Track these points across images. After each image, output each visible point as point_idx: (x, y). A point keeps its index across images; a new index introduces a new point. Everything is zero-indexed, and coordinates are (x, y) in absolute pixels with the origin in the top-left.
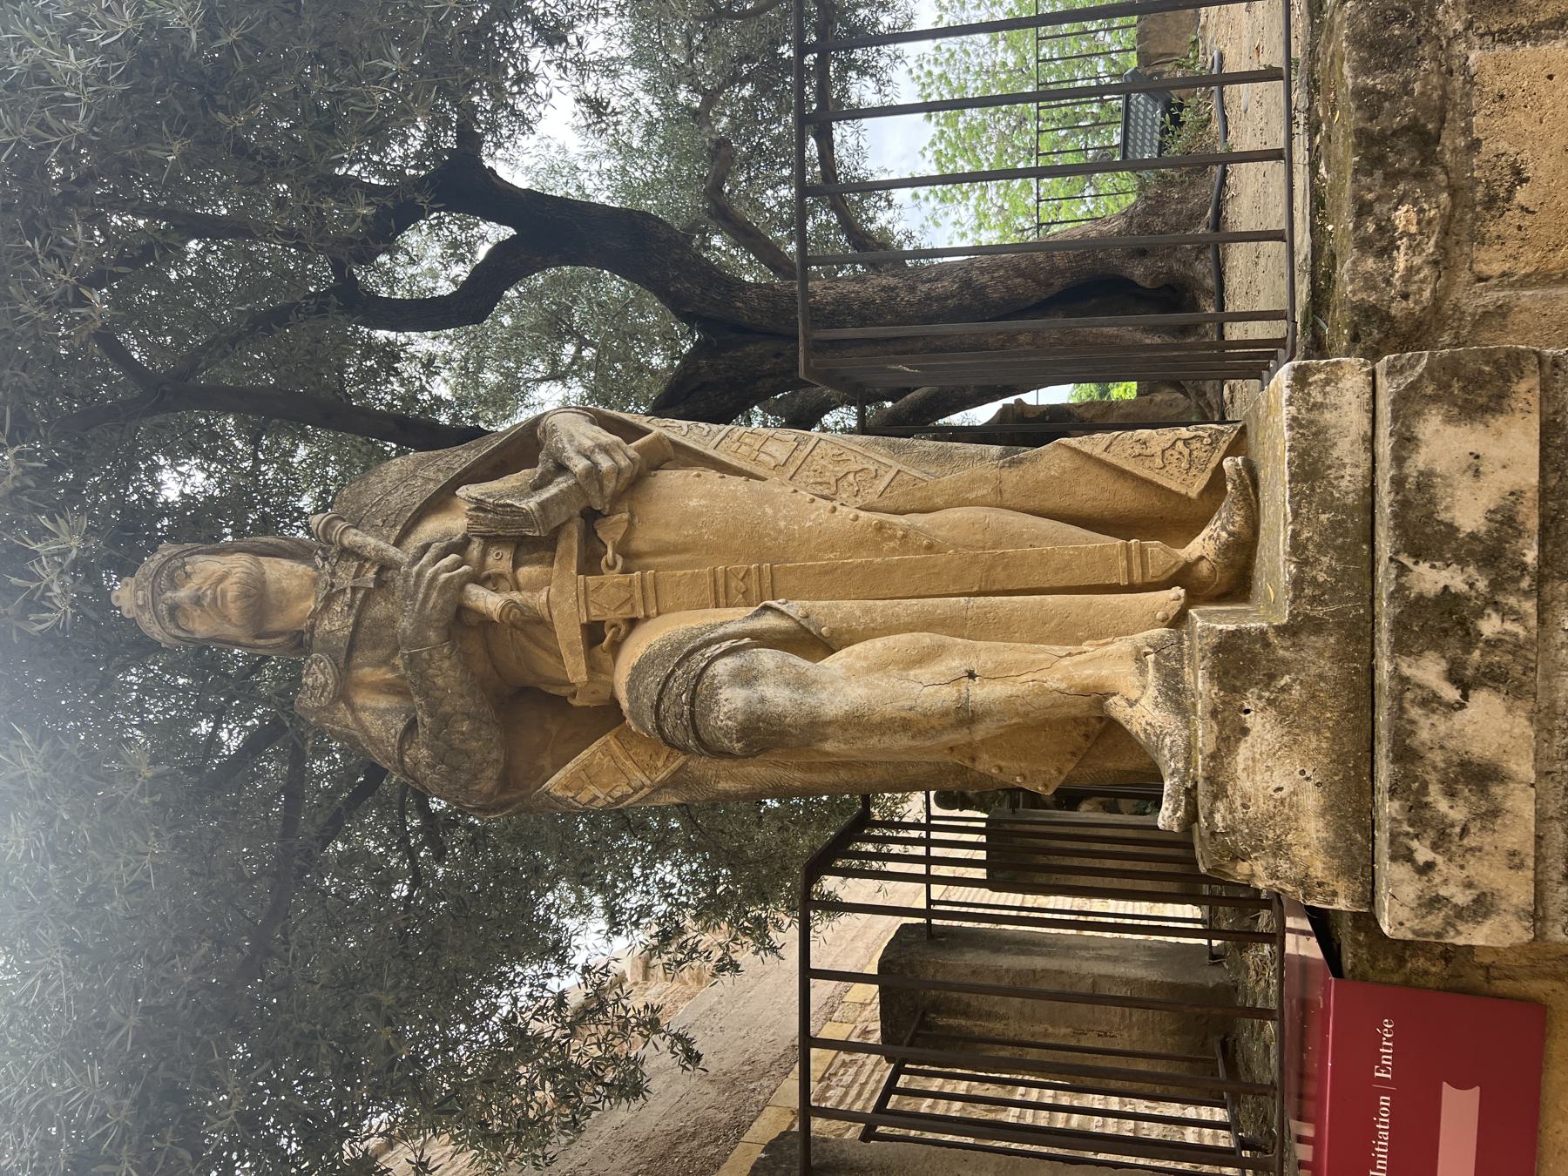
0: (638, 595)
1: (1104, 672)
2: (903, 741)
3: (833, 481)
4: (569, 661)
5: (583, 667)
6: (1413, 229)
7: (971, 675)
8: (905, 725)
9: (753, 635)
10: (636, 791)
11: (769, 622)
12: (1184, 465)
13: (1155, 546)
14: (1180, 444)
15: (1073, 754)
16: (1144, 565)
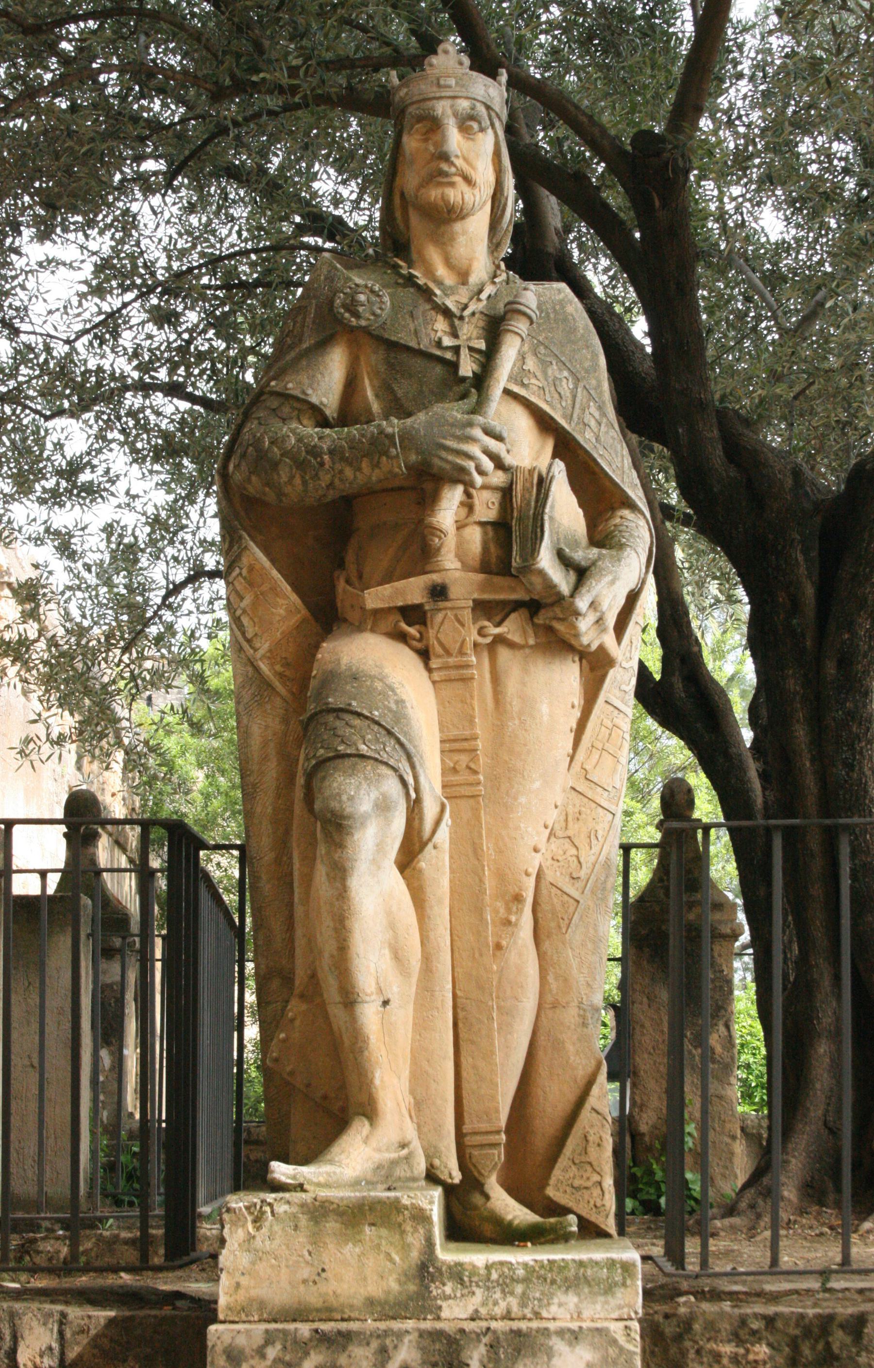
0: (451, 661)
1: (389, 1117)
2: (329, 947)
3: (570, 833)
4: (387, 590)
5: (380, 605)
6: (751, 1357)
7: (386, 1003)
8: (343, 949)
9: (418, 801)
10: (249, 641)
11: (430, 809)
12: (577, 1183)
13: (499, 1155)
14: (596, 1178)
15: (308, 1085)
16: (482, 1146)
